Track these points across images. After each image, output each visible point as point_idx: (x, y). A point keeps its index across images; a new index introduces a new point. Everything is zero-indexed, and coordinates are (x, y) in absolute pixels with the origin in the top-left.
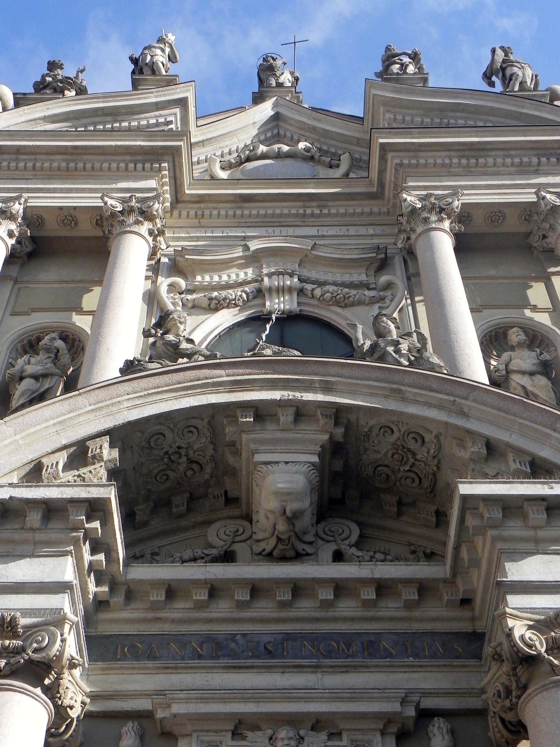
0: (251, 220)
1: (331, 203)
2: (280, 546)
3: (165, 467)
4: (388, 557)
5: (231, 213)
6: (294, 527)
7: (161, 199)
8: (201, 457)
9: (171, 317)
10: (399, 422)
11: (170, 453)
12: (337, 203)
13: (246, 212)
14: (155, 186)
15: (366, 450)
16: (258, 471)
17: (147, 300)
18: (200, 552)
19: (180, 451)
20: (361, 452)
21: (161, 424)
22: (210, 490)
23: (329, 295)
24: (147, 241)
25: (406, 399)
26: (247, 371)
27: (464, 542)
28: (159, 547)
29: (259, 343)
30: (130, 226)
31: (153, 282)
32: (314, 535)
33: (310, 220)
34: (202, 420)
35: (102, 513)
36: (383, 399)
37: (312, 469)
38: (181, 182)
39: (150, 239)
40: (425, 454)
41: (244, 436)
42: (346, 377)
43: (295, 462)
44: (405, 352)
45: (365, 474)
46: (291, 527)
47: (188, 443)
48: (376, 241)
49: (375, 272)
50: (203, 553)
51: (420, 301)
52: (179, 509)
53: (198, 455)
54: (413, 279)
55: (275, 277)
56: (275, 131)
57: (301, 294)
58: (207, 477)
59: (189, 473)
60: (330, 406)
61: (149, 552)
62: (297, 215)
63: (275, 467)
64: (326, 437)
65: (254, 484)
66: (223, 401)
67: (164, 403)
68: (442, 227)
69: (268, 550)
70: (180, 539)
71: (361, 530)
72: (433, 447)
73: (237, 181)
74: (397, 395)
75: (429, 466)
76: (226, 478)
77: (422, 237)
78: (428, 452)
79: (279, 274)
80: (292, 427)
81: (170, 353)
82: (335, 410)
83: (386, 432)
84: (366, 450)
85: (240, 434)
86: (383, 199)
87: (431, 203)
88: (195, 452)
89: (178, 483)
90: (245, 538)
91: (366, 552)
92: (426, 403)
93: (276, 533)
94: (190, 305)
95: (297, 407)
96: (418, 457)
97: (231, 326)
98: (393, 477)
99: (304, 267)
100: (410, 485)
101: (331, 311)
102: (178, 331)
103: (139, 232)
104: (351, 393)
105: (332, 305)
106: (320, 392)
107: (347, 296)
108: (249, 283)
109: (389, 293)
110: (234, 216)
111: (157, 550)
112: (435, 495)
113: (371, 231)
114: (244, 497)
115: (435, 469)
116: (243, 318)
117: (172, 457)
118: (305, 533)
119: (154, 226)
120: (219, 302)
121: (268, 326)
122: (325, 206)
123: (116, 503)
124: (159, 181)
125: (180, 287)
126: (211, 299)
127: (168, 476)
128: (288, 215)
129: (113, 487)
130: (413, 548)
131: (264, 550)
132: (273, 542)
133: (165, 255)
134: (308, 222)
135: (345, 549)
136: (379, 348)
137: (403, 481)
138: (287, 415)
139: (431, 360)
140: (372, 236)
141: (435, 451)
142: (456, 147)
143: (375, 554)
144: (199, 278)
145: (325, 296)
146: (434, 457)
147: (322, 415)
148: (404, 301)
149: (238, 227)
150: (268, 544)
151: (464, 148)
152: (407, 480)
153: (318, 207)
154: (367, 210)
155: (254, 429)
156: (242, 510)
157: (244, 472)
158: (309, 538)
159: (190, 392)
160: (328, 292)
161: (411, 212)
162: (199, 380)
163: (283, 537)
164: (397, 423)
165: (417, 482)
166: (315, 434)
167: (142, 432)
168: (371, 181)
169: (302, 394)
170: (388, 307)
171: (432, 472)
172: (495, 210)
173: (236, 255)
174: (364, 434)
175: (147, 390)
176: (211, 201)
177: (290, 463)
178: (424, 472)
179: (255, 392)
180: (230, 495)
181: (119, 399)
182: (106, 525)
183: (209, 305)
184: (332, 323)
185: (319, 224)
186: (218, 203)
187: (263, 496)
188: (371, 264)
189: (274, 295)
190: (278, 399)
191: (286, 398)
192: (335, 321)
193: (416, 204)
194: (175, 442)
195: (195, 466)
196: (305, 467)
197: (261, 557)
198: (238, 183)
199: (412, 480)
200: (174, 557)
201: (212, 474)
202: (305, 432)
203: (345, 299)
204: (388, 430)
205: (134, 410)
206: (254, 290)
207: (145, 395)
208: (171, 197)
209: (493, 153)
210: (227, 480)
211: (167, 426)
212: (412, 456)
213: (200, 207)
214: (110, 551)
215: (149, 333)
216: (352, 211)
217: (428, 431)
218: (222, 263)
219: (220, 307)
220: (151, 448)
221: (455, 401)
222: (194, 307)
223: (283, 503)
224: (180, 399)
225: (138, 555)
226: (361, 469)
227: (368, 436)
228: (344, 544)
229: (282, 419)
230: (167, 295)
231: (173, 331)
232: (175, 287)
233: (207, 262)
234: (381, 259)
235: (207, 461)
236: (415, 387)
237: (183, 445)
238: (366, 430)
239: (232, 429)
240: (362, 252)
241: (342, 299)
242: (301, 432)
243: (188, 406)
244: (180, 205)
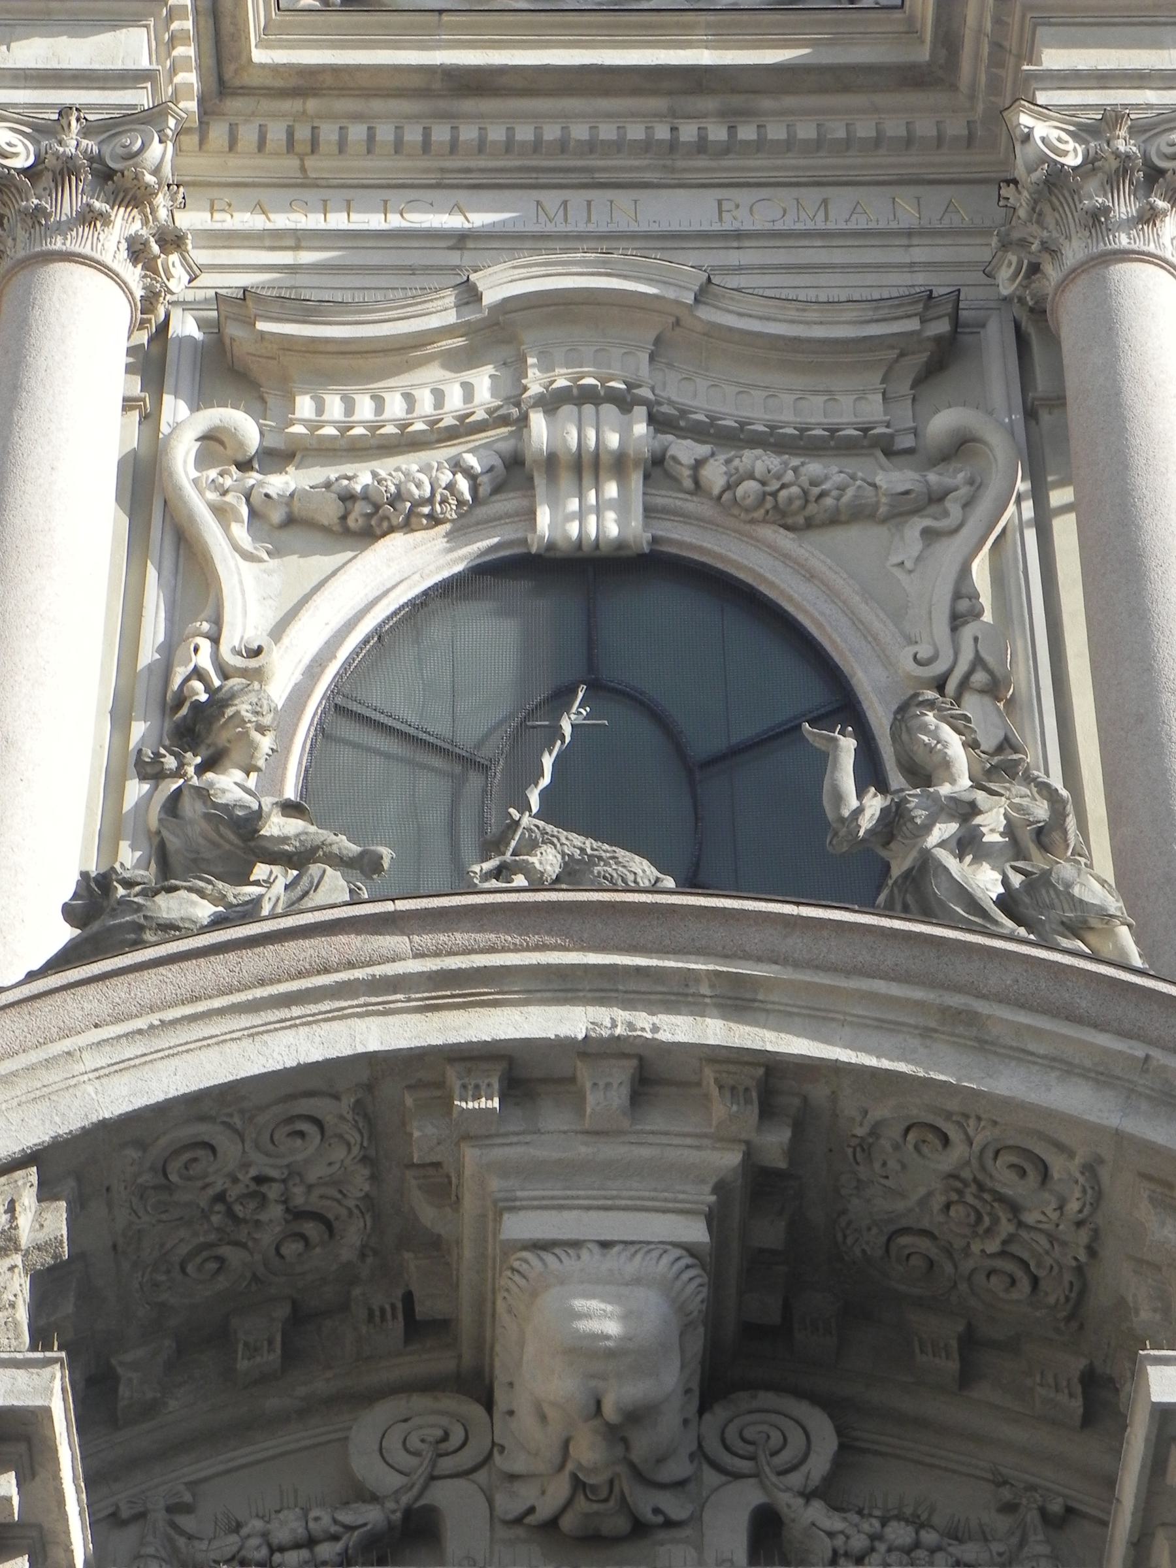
0: (482, 163)
1: (767, 103)
2: (581, 1504)
3: (213, 1237)
4: (929, 1537)
5: (413, 135)
6: (627, 1448)
7: (172, 122)
8: (329, 1203)
9: (230, 712)
10: (966, 1116)
11: (233, 1193)
12: (790, 101)
13: (469, 133)
14: (144, 63)
15: (860, 1185)
16: (513, 1270)
17: (128, 495)
18: (326, 1520)
19: (264, 1189)
20: (843, 1192)
21: (202, 1118)
22: (357, 1291)
23: (750, 486)
24: (123, 285)
25: (992, 1043)
26: (483, 938)
27: (1163, 1524)
28: (191, 1485)
29: (517, 823)
30: (62, 229)
31: (145, 418)
32: (692, 1457)
34: (336, 1097)
35: (22, 1447)
36: (916, 1042)
37: (688, 1267)
38: (234, 24)
39: (133, 275)
40: (1049, 1211)
41: (471, 1155)
42: (797, 965)
43: (632, 1243)
44: (996, 838)
45: (857, 1251)
46: (619, 1451)
47: (288, 1166)
48: (921, 279)
49: (916, 384)
50: (335, 1521)
51: (1065, 509)
52: (258, 1359)
53: (322, 1197)
54: (1045, 417)
55: (568, 410)
57: (657, 473)
58: (347, 1254)
59: (291, 1249)
60: (746, 1059)
61: (162, 1504)
62: (647, 146)
63: (569, 1263)
64: (731, 1158)
65: (501, 1306)
66: (403, 1044)
67: (213, 1054)
68: (1152, 248)
69: (545, 1511)
70: (259, 1456)
71: (839, 1432)
72: (1077, 1194)
73: (434, 18)
74: (960, 1029)
75: (1064, 1244)
76: (407, 1255)
77: (1083, 280)
78: (1061, 1208)
79: (583, 397)
80: (626, 1124)
81: (227, 847)
82: (761, 1071)
83: (924, 1141)
84: (860, 1185)
85: (457, 1144)
86: (954, 87)
87: (1117, 154)
88: (310, 1187)
89: (255, 1278)
90: (469, 1465)
91: (855, 1518)
92: (1054, 1059)
93: (570, 1466)
94: (277, 516)
95: (641, 1058)
96: (1030, 1218)
97: (417, 597)
98: (949, 1268)
99: (670, 365)
100: (1002, 1295)
101: (759, 543)
102: (252, 757)
103: (97, 256)
104: (810, 1016)
105: (764, 521)
106: (715, 1012)
107: (816, 491)
108: (481, 427)
109: (961, 476)
110: (426, 146)
111: (187, 1498)
112: (1081, 1327)
113: (907, 214)
114: (466, 1318)
115: (1083, 1257)
116: (459, 568)
117: (238, 1209)
118: (661, 1461)
119: (145, 222)
120: (377, 507)
121: (548, 761)
122: (746, 114)
123: (66, 1410)
124: (163, 54)
125: (241, 445)
126: (348, 498)
127: (221, 1260)
128: (619, 146)
129: (58, 1366)
130: (1006, 1494)
131: (531, 1510)
132: (559, 1489)
133: (186, 305)
134: (685, 170)
135: (789, 1506)
136: (909, 825)
137: (980, 1278)
138: (608, 1085)
139: (1076, 891)
140: (909, 233)
141: (1084, 1205)
143: (883, 1525)
144: (304, 406)
145: (740, 491)
146: (1079, 1224)
147: (721, 1087)
148: (1011, 508)
149: (438, 186)
150: (543, 1493)
152: (993, 1279)
153: (723, 114)
154: (894, 128)
155: (502, 1130)
156: (460, 1357)
157: (468, 1253)
158: (677, 1468)
159: (296, 1011)
160: (751, 477)
161: (1046, 182)
162: (326, 971)
163: (591, 1480)
164: (959, 1118)
165: (1024, 1284)
166: (698, 1148)
167: (141, 1145)
168: (911, 20)
169: (655, 1019)
170: (955, 531)
171: (1074, 1264)
173: (434, 322)
174: (854, 1142)
175: (160, 1009)
176: (343, 91)
177: (616, 1249)
178: (1048, 1261)
179: (507, 1011)
180: (422, 1310)
181: (67, 1044)
182: (34, 1475)
183: (344, 518)
184: (762, 588)
185: (722, 177)
186: (368, 96)
187: (530, 1350)
188: (902, 355)
189: (566, 480)
190: (581, 1036)
191: (605, 1033)
192: (772, 585)
193: (1065, 153)
194: (246, 1166)
195: (311, 1229)
196: (665, 1260)
197: (520, 1532)
198: (439, 25)
199: (1008, 1280)
200: (244, 1531)
201: (363, 1246)
202: (664, 1140)
203: (807, 501)
204: (930, 1137)
205: (116, 1079)
206: (497, 462)
207: (152, 1027)
208: (201, 77)
210: (412, 1263)
211: (224, 1123)
212: (1010, 1216)
213: (304, 113)
214: (44, 1546)
215: (157, 769)
216: (841, 134)
217: (1060, 1147)
218: (385, 351)
219: (379, 525)
220: (169, 1188)
221: (1147, 1058)
222: (291, 521)
223: (593, 1383)
224: (265, 1037)
225: (125, 1513)
226: (845, 1237)
227: (865, 1147)
228: (788, 1489)
229: (592, 1100)
230: (194, 474)
231: (236, 755)
232: (222, 443)
233: (330, 348)
234: (938, 339)
235: (351, 1213)
236: (1022, 1006)
237: (274, 1173)
238: (860, 1132)
239: (430, 1130)
241: (798, 503)
242: (651, 1139)
243: (291, 1063)
244: (234, 104)
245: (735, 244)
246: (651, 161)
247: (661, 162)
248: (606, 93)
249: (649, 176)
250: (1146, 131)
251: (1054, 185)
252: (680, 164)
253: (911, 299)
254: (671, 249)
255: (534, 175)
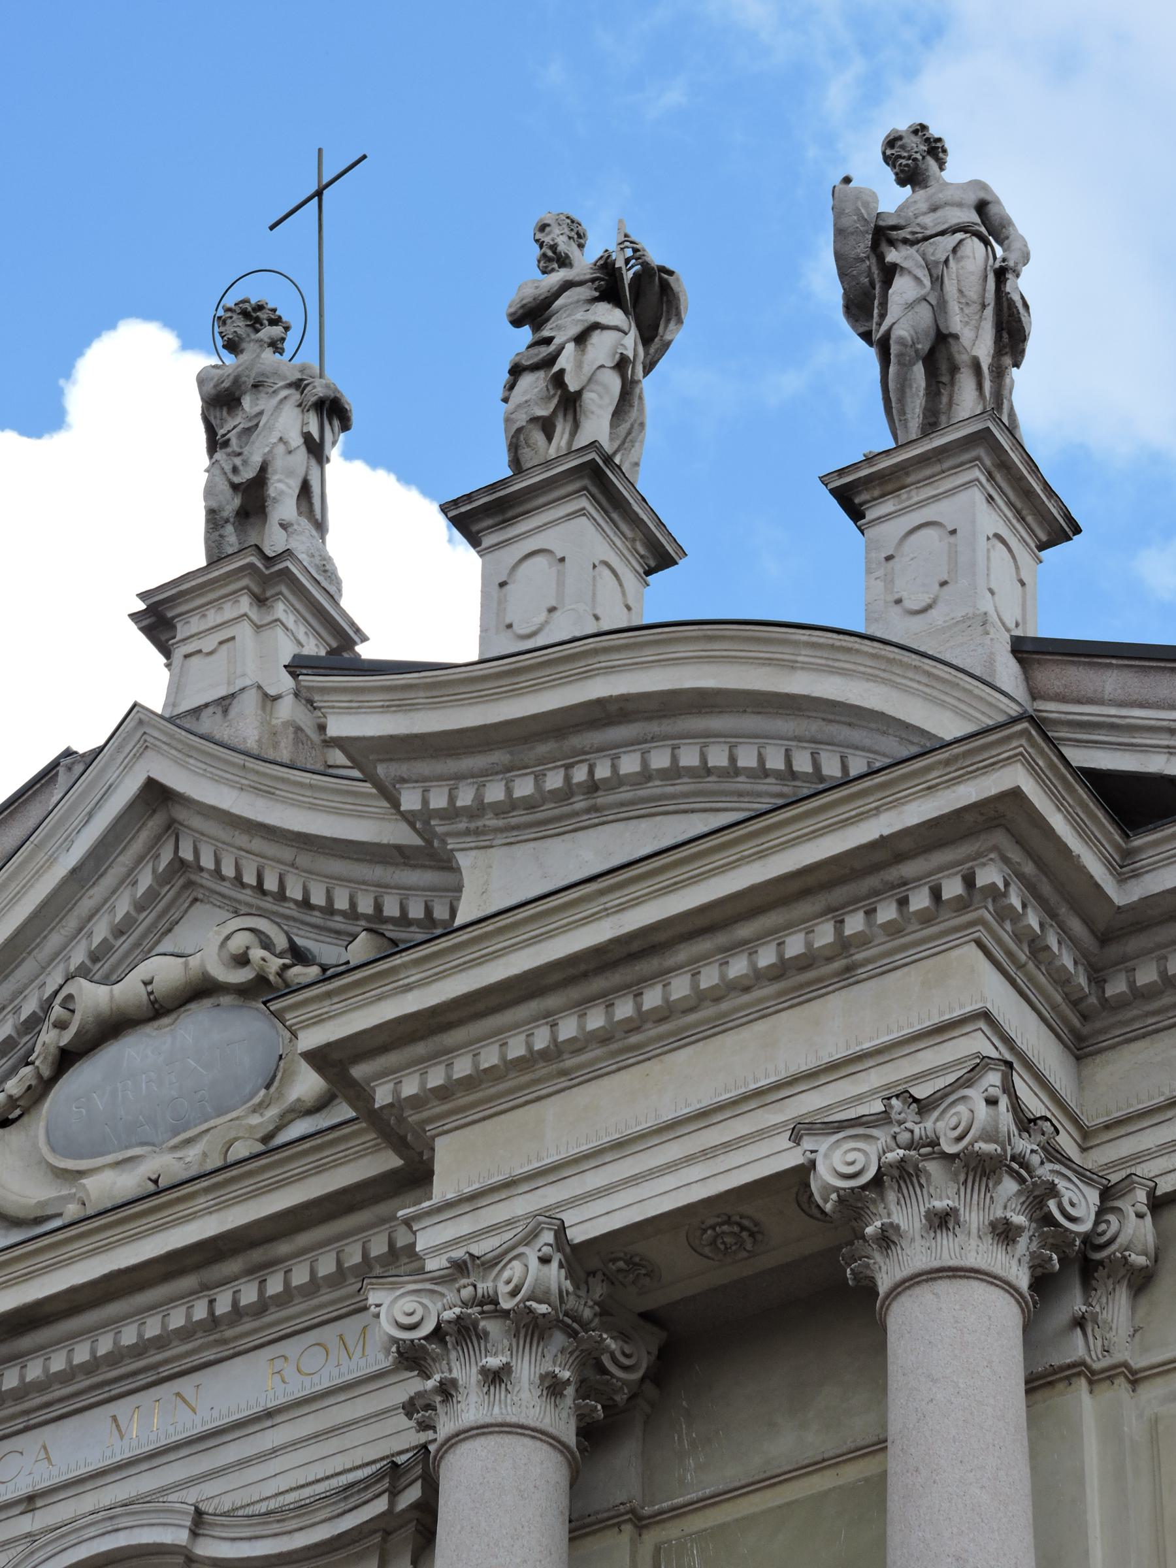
1: (283, 1248)
33: (238, 1330)
56: (166, 857)
122: (269, 1265)
134: (236, 1338)
142: (557, 977)
151: (583, 967)
153: (251, 1271)
172: (712, 1221)
209: (683, 953)
234: (415, 1506)
240: (343, 1506)
245: (269, 1423)
246: (202, 1340)
247: (212, 1338)
248: (141, 1287)
249: (208, 1355)
250: (497, 1264)
251: (416, 1358)
252: (229, 1333)
253: (377, 1478)
254: (215, 1446)
255: (107, 1389)
